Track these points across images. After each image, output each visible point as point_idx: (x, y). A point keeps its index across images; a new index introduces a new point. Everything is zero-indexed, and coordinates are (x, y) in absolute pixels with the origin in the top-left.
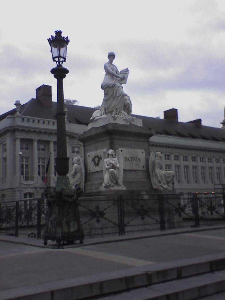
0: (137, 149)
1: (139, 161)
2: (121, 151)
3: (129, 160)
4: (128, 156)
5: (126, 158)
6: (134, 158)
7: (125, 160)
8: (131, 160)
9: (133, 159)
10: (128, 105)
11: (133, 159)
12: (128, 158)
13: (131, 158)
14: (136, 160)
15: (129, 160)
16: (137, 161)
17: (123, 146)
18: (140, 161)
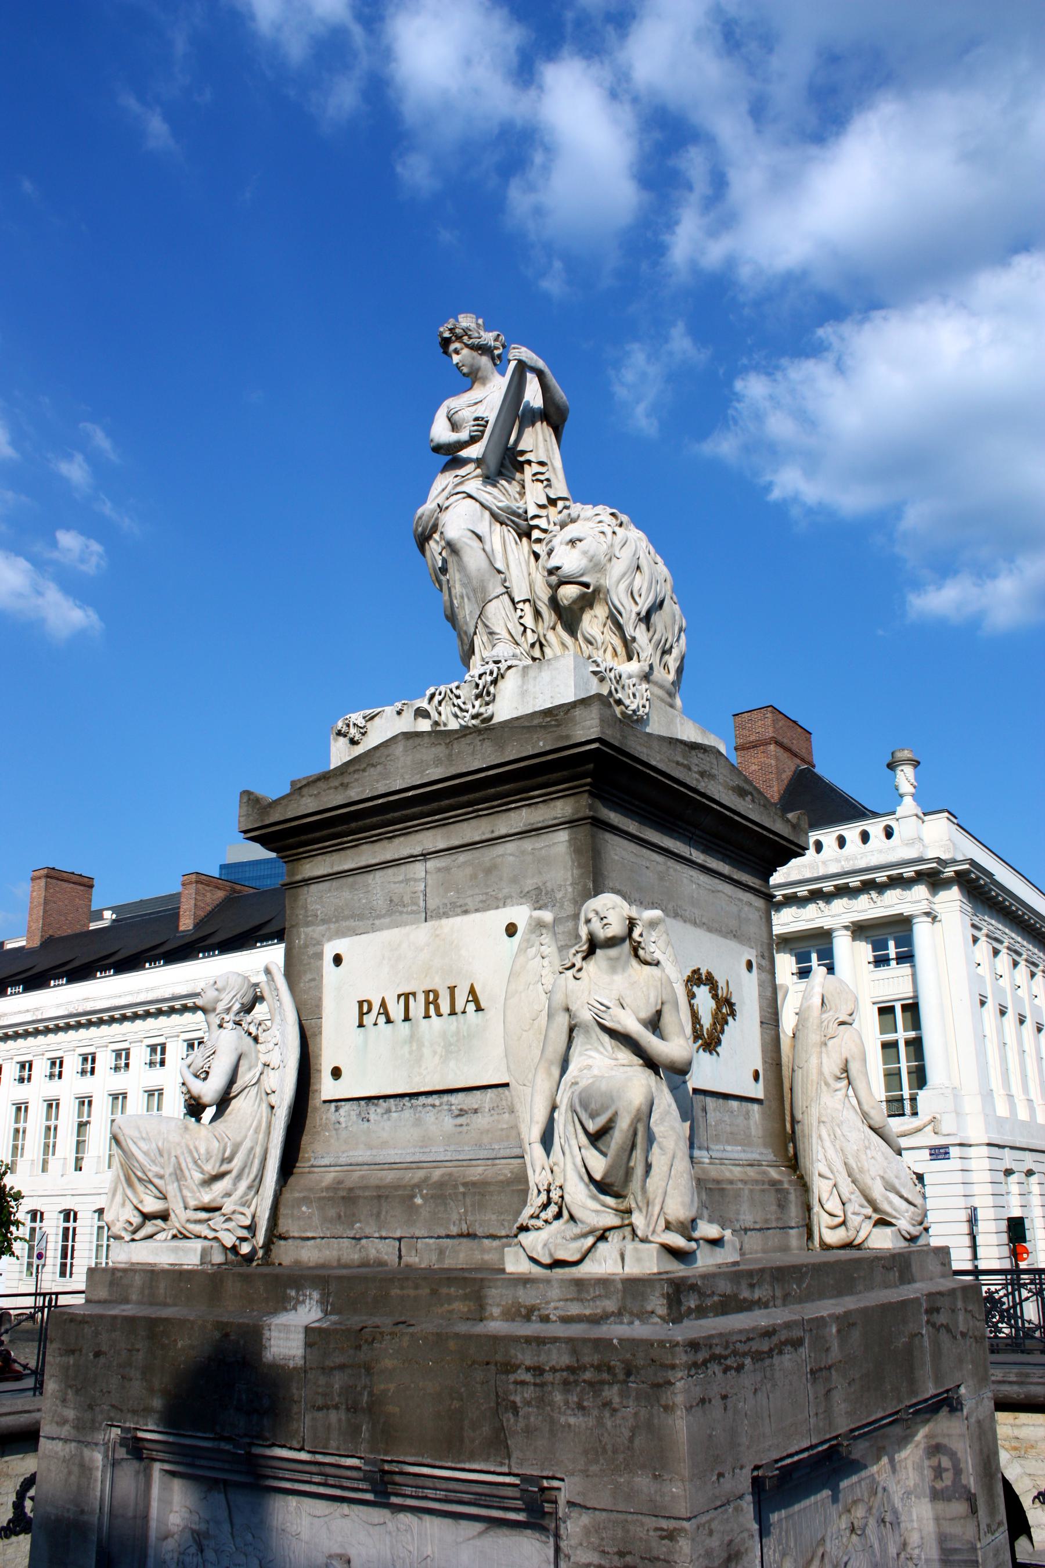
0: (466, 912)
1: (471, 1007)
2: (338, 960)
3: (389, 1021)
4: (381, 989)
5: (364, 1007)
6: (432, 999)
7: (361, 1025)
8: (407, 1019)
9: (417, 1008)
10: (562, 583)
11: (417, 1008)
12: (383, 1004)
13: (407, 996)
14: (445, 1008)
15: (389, 1021)
16: (453, 1013)
17: (359, 920)
18: (479, 1009)
